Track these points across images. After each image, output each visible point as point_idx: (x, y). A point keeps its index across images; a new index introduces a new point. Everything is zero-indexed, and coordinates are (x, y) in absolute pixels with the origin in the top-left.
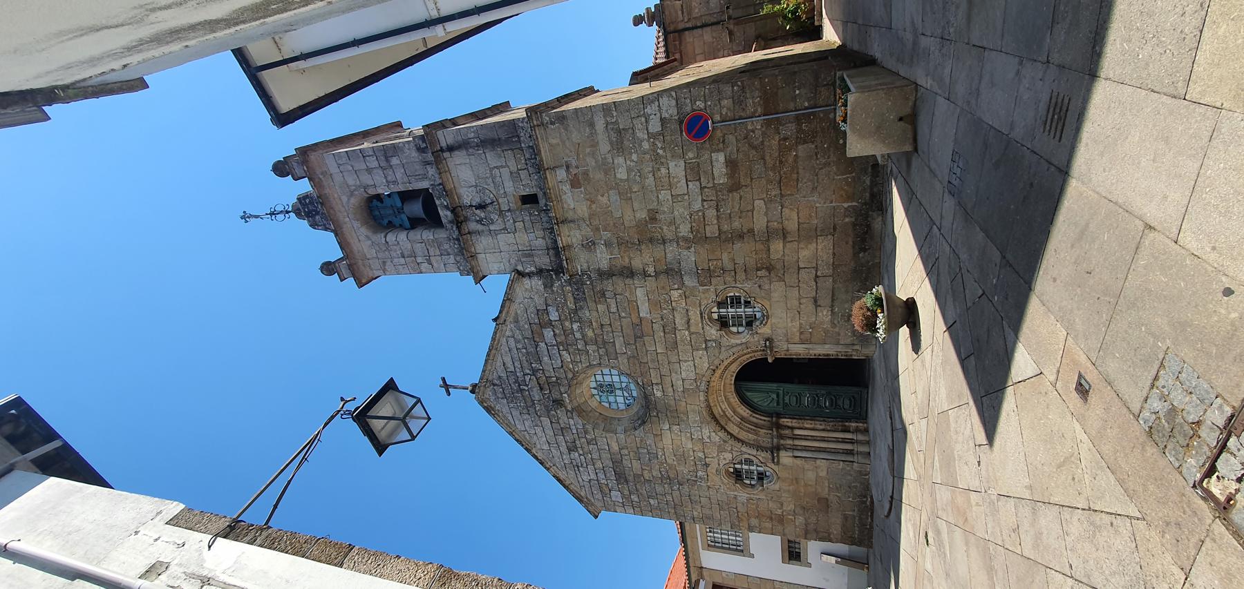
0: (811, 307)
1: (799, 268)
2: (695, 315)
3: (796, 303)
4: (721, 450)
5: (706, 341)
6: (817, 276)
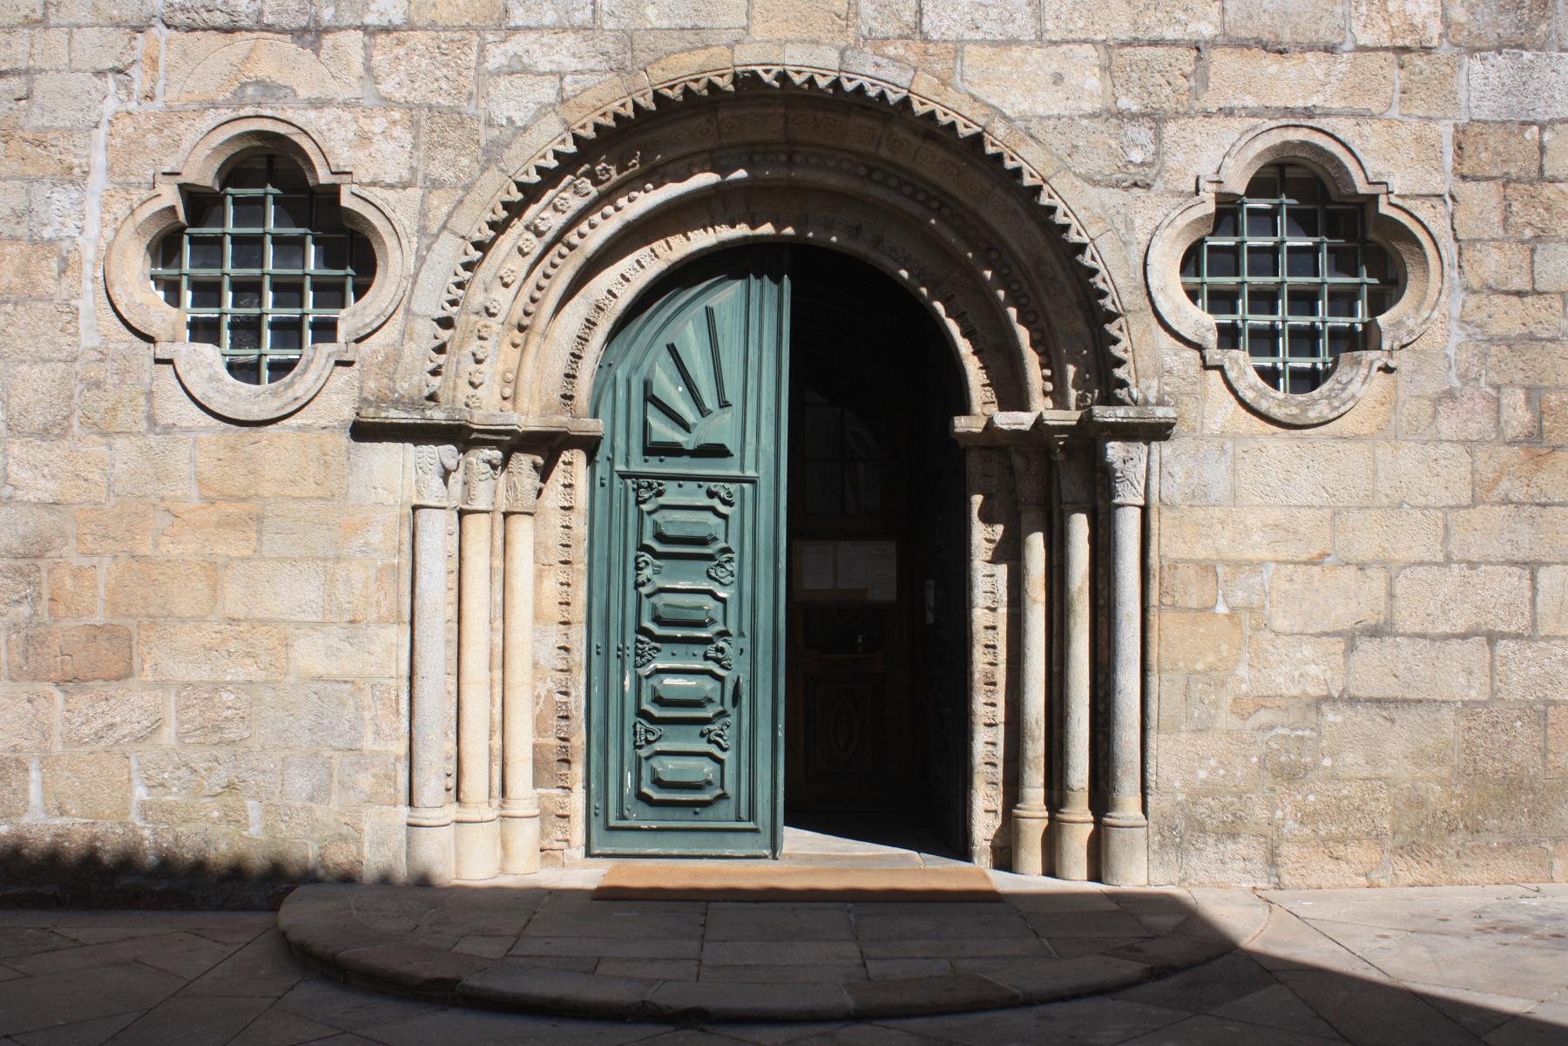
0: (1344, 614)
1: (1532, 567)
2: (1297, 83)
3: (1365, 548)
4: (430, 122)
5: (1155, 118)
6: (1492, 638)
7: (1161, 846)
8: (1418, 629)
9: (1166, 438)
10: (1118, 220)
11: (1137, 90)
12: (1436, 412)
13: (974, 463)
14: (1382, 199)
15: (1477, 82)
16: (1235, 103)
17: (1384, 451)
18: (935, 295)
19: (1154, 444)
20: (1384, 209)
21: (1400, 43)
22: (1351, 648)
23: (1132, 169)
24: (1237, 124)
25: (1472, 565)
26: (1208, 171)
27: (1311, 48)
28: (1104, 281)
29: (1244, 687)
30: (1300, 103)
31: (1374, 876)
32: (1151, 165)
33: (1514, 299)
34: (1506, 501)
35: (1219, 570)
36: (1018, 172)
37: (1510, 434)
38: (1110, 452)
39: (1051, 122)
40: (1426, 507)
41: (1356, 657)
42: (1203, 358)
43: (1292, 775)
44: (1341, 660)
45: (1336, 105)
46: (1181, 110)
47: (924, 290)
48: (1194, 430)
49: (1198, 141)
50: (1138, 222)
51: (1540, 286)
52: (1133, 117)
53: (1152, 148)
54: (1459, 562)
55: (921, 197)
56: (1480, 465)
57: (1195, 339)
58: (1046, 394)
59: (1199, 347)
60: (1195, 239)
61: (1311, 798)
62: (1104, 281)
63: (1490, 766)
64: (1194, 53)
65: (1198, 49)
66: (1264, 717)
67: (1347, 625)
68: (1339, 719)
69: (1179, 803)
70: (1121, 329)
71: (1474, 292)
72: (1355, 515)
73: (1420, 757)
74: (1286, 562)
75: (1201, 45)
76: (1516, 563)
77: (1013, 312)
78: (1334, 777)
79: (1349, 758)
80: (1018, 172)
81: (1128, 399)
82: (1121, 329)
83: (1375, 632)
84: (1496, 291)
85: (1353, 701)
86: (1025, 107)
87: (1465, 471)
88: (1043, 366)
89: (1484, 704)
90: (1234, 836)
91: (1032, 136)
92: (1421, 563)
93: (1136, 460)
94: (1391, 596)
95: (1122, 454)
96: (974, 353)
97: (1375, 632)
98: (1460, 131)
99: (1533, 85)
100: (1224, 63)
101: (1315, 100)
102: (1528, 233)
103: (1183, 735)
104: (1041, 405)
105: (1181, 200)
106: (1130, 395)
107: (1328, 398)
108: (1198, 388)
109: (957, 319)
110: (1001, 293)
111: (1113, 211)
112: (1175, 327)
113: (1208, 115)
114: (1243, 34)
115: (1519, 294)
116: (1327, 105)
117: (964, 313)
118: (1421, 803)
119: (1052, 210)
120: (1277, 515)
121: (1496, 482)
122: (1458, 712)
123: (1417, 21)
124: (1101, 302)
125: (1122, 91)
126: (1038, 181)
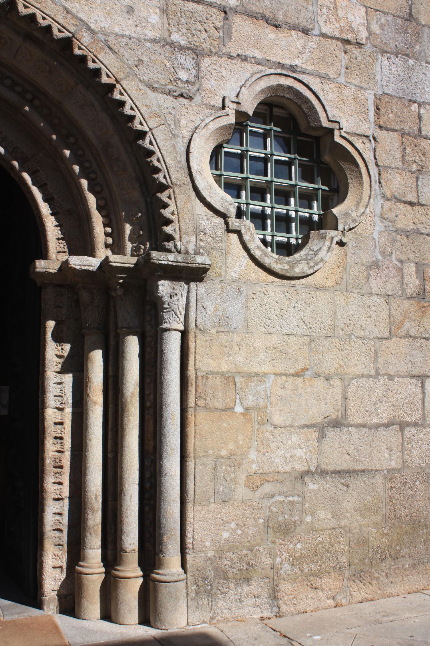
0: (319, 410)
3: (329, 366)
5: (197, 53)
6: (402, 426)
7: (197, 594)
8: (361, 421)
9: (201, 280)
10: (170, 118)
11: (184, 31)
12: (369, 274)
13: (49, 297)
14: (337, 133)
15: (385, 71)
16: (248, 53)
17: (340, 299)
18: (23, 168)
19: (193, 285)
20: (337, 139)
21: (345, 37)
22: (322, 436)
23: (180, 84)
24: (249, 68)
25: (391, 377)
26: (231, 95)
27: (294, 28)
28: (159, 160)
29: (254, 467)
30: (288, 62)
31: (338, 597)
32: (193, 84)
33: (409, 207)
34: (408, 336)
35: (237, 379)
36: (97, 72)
37: (409, 292)
38: (160, 288)
39: (124, 40)
40: (364, 338)
41: (326, 442)
42: (227, 224)
43: (285, 530)
44: (315, 443)
45: (309, 68)
46: (213, 50)
47: (16, 164)
48: (220, 275)
49: (224, 74)
50: (183, 122)
51: (422, 201)
52: (182, 48)
53: (194, 72)
54: (384, 375)
55: (18, 89)
56: (393, 311)
57: (222, 210)
58: (107, 246)
59: (224, 216)
60: (216, 144)
61: (299, 546)
62: (159, 160)
63: (402, 512)
64: (223, 14)
65: (225, 12)
66: (267, 488)
67: (319, 419)
68: (315, 487)
69: (209, 559)
70: (169, 197)
71: (388, 200)
72: (324, 342)
73: (364, 510)
74: (280, 375)
75: (228, 11)
76: (413, 376)
77: (84, 183)
78: (312, 530)
79: (322, 514)
80: (97, 72)
81: (173, 249)
82: (169, 197)
83: (337, 424)
84: (399, 201)
85: (324, 473)
86: (105, 25)
87: (385, 314)
88: (105, 225)
89: (399, 470)
90: (248, 580)
91: (109, 47)
92: (362, 376)
93: (179, 296)
94: (345, 398)
95: (170, 290)
96: (52, 214)
97: (337, 424)
98: (378, 98)
99: (414, 79)
100: (241, 25)
101: (296, 62)
102: (415, 167)
103: (212, 506)
104: (102, 253)
105: (213, 111)
106: (175, 247)
107: (306, 259)
108: (223, 245)
109: (40, 188)
110: (77, 168)
111: (166, 111)
112: (208, 199)
113: (230, 57)
114: (254, 9)
115: (411, 204)
116: (304, 66)
117: (45, 184)
118: (365, 542)
119: (122, 104)
120: (274, 340)
121: (402, 322)
122: (385, 477)
123: (354, 26)
124: (155, 176)
125: (175, 29)
126: (112, 81)
